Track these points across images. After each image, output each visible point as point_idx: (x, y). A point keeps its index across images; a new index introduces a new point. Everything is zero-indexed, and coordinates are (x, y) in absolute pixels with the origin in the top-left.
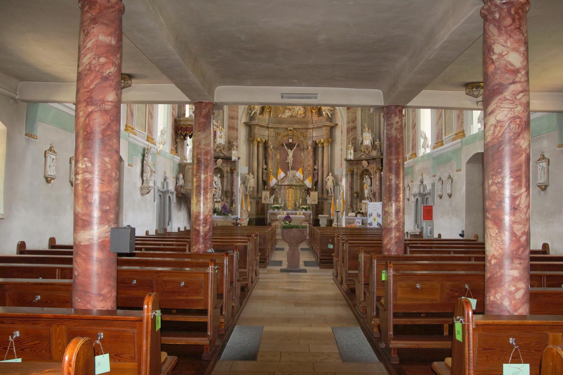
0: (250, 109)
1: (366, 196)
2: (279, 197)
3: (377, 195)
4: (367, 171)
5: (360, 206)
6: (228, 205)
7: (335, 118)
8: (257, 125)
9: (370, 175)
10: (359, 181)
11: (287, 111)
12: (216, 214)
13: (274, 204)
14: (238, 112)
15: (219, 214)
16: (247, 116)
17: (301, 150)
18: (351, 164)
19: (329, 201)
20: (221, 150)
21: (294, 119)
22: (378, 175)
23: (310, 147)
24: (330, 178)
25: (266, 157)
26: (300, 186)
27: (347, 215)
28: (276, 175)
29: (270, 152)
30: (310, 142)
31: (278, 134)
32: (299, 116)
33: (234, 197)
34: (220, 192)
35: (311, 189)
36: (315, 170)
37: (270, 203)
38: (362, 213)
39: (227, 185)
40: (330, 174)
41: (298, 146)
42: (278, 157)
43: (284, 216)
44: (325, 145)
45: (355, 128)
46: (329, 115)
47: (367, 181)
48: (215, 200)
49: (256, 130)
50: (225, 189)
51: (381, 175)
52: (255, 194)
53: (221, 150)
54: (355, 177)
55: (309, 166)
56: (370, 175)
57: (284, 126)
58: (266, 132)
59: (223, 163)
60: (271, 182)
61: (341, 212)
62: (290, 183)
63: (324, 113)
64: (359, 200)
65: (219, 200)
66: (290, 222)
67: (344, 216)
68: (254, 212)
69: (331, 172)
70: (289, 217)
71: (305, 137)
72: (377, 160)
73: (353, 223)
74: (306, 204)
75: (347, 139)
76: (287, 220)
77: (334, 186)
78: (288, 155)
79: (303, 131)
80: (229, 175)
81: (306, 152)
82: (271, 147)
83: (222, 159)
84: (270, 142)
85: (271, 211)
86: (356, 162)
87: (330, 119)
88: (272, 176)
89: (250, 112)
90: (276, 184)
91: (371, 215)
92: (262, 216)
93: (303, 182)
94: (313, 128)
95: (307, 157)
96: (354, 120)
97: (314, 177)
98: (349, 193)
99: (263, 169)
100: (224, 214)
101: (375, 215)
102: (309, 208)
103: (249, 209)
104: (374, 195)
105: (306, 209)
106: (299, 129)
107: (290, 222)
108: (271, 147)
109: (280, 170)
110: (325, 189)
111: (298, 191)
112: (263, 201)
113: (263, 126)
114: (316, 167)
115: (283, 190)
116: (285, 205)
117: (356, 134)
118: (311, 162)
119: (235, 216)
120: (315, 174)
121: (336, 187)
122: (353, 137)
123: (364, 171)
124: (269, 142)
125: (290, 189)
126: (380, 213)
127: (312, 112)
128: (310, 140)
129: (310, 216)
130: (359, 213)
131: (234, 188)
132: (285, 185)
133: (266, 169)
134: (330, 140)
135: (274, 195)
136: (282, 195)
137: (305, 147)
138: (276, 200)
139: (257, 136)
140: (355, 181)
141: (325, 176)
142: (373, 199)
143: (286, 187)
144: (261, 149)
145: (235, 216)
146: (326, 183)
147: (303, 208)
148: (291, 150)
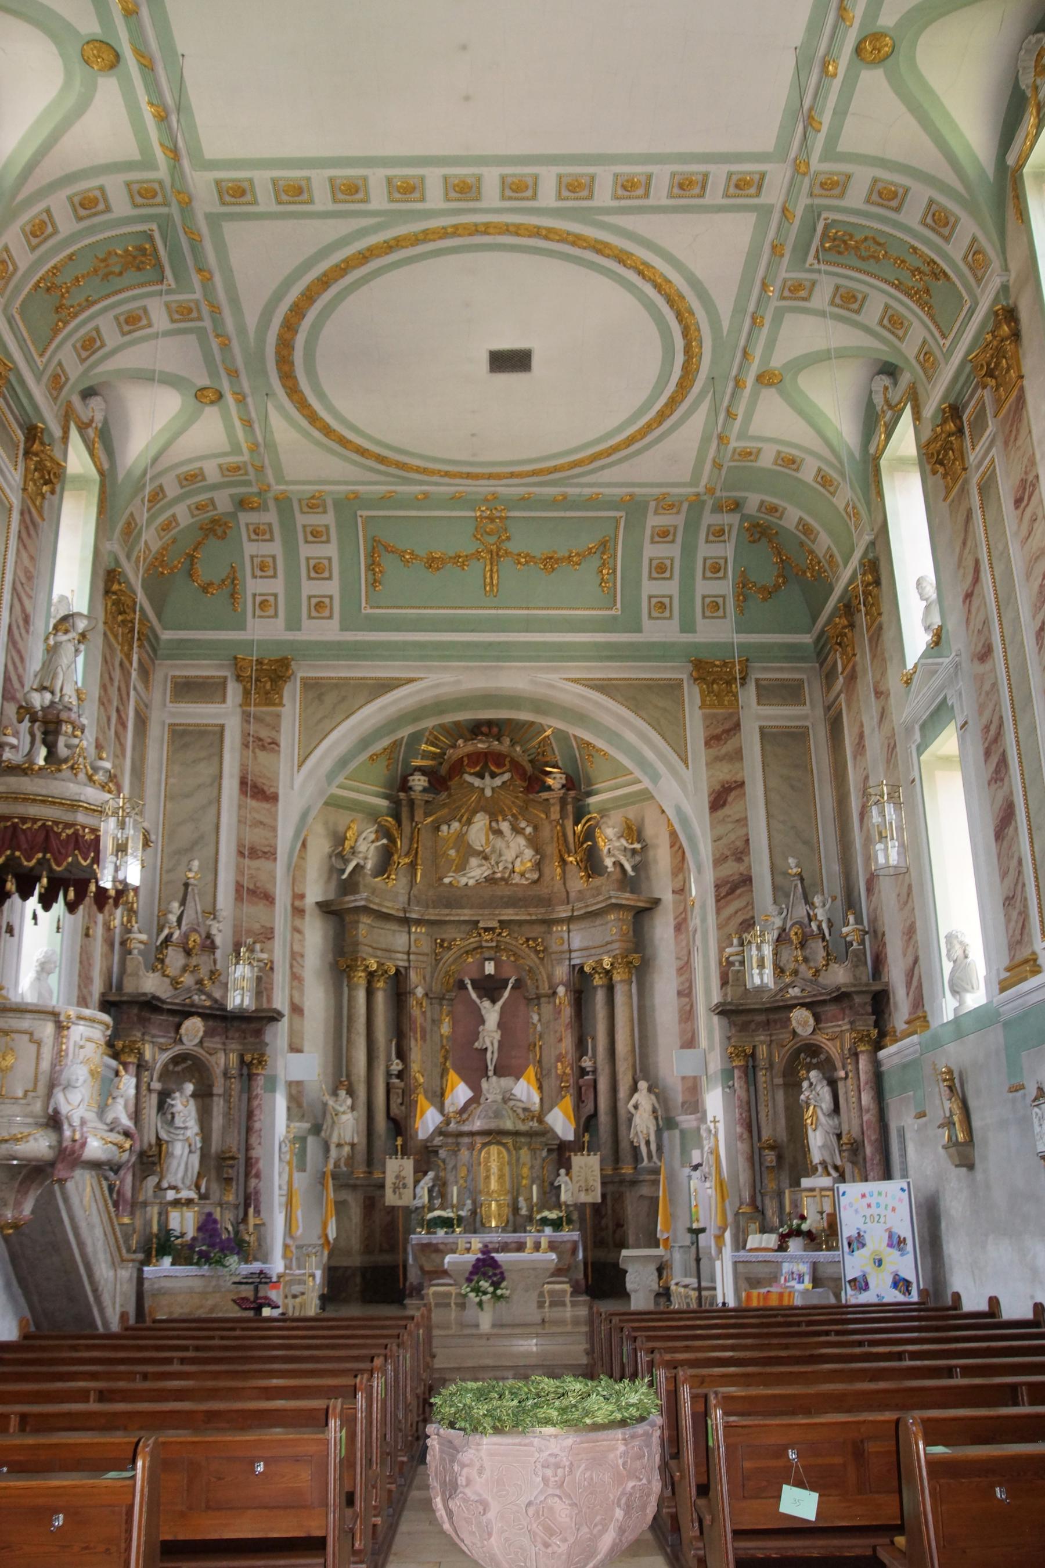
0: (340, 856)
1: (816, 1156)
2: (451, 1178)
3: (869, 1150)
4: (813, 1050)
5: (796, 1204)
6: (226, 1221)
7: (648, 878)
8: (366, 910)
9: (827, 1068)
10: (780, 1096)
11: (474, 861)
12: (167, 1261)
13: (431, 1209)
14: (274, 829)
15: (184, 1255)
16: (329, 879)
17: (529, 1000)
18: (744, 1028)
19: (645, 1190)
20: (200, 982)
21: (501, 890)
22: (863, 1062)
23: (561, 990)
24: (643, 1099)
25: (400, 1033)
26: (530, 1134)
27: (740, 1244)
28: (438, 1098)
29: (416, 1012)
30: (561, 972)
31: (443, 945)
32: (516, 879)
33: (253, 1182)
34: (195, 1159)
35: (577, 1146)
36: (583, 1072)
37: (418, 1203)
38: (810, 1235)
39: (225, 1129)
40: (643, 1085)
41: (518, 985)
42: (446, 1029)
43: (471, 1258)
44: (616, 977)
45: (747, 880)
47: (816, 1093)
48: (171, 1195)
49: (362, 930)
50: (215, 1147)
51: (876, 1064)
52: (360, 1172)
53: (200, 982)
54: (762, 1076)
55: (560, 1058)
56: (827, 1068)
57: (466, 914)
58: (399, 940)
59: (209, 1033)
60: (418, 1124)
61: (712, 1231)
62: (492, 1125)
63: (608, 862)
64: (785, 1182)
65: (185, 1194)
66: (496, 1285)
67: (728, 1251)
68: (355, 1243)
69: (646, 1078)
70: (494, 1264)
71: (543, 953)
72: (857, 1000)
73: (774, 1279)
74: (558, 1205)
75: (720, 927)
76: (485, 1276)
77: (659, 1132)
78: (482, 1021)
79: (537, 931)
80: (236, 1085)
81: (547, 1009)
82: (420, 992)
83: (204, 1016)
84: (414, 977)
85: (419, 1236)
86: (761, 1018)
87: (629, 882)
88: (422, 1100)
89: (340, 865)
90: (440, 1132)
91: (857, 1242)
92: (386, 1258)
93: (541, 1121)
94: (570, 920)
95: (552, 1026)
96: (741, 852)
97: (579, 1100)
98: (742, 1147)
99: (389, 1074)
100: (205, 1258)
101: (876, 1241)
102: (570, 1221)
103: (332, 1234)
104: (855, 1149)
105: (557, 1225)
106: (520, 923)
107: (496, 1285)
108: (420, 992)
109: (452, 1076)
110: (624, 1145)
111: (525, 1154)
112: (391, 1198)
114: (587, 1063)
115: (464, 1154)
116: (474, 1212)
117: (750, 904)
118: (567, 1045)
119: (256, 1266)
120: (582, 1088)
121: (666, 1134)
122: (740, 918)
123: (798, 1052)
124: (413, 975)
125: (494, 1149)
126: (904, 1229)
127: (563, 862)
128: (560, 961)
129: (574, 1251)
130: (798, 1233)
131: (253, 1140)
132: (472, 1134)
133: (400, 1075)
134: (635, 958)
135: (431, 1174)
136: (463, 1172)
137: (545, 988)
138: (439, 1190)
139: (364, 951)
140: (762, 1098)
141: (622, 1094)
142: (848, 1168)
143: (479, 1140)
144: (380, 999)
145: (256, 1266)
146: (630, 1119)
147: (545, 1222)
148: (494, 1002)
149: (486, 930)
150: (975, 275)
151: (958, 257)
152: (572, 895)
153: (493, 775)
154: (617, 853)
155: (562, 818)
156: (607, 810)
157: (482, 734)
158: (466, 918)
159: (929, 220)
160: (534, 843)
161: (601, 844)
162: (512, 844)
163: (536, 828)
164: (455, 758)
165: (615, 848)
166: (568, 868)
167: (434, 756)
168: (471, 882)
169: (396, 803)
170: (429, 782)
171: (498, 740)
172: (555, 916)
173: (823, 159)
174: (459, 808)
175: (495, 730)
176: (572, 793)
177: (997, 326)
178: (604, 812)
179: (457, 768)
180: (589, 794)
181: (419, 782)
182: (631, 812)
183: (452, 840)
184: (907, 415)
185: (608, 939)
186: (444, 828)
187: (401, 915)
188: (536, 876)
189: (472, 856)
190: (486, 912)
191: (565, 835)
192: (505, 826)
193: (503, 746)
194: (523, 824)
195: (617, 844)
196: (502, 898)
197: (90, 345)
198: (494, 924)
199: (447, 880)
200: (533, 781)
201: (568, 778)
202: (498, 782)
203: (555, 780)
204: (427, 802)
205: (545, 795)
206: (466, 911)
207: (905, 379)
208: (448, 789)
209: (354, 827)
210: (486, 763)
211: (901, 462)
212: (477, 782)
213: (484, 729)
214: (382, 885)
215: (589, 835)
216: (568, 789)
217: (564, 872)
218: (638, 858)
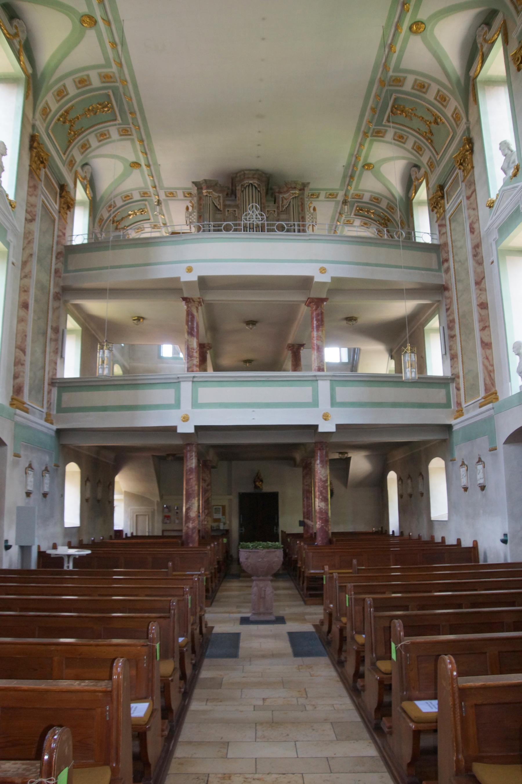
150: (456, 124)
151: (449, 115)
159: (438, 98)
173: (393, 71)
177: (464, 146)
184: (424, 184)
197: (85, 147)
207: (422, 171)
211: (421, 203)
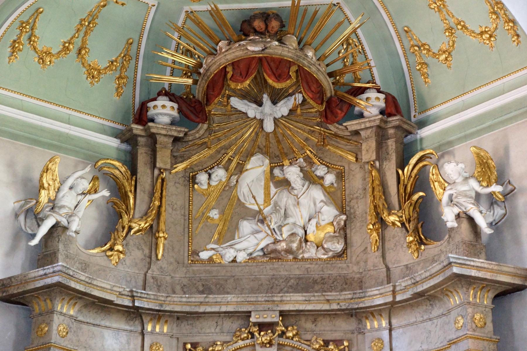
11: (246, 226)
21: (288, 269)
32: (311, 252)
46: (481, 222)
57: (230, 302)
63: (449, 215)
79: (342, 328)
94: (392, 308)
106: (315, 316)
113: (103, 306)
127: (382, 222)
149: (263, 326)
152: (396, 272)
153: (276, 98)
154: (462, 200)
155: (378, 158)
156: (450, 143)
157: (256, 32)
158: (230, 309)
160: (339, 199)
161: (438, 190)
162: (302, 200)
163: (340, 176)
164: (214, 69)
165: (460, 194)
166: (390, 232)
167: (188, 72)
168: (242, 257)
169: (128, 139)
170: (180, 110)
171: (280, 41)
172: (368, 303)
174: (227, 148)
175: (274, 24)
176: (395, 120)
178: (444, 149)
179: (218, 84)
180: (422, 124)
181: (164, 111)
182: (488, 143)
183: (214, 195)
185: (453, 336)
186: (202, 178)
187: (127, 302)
188: (339, 247)
189: (244, 218)
190: (261, 298)
191: (383, 185)
192: (293, 173)
193: (287, 50)
194: (321, 171)
195: (465, 188)
196: (287, 279)
198: (273, 317)
199: (204, 255)
200: (336, 104)
201: (390, 100)
202: (283, 108)
203: (371, 104)
204: (176, 140)
205: (353, 125)
206: (230, 298)
208: (205, 118)
209: (56, 168)
210: (263, 76)
212: (251, 110)
213: (258, 24)
214: (103, 261)
215: (421, 182)
216: (390, 115)
217: (383, 239)
218: (499, 211)
